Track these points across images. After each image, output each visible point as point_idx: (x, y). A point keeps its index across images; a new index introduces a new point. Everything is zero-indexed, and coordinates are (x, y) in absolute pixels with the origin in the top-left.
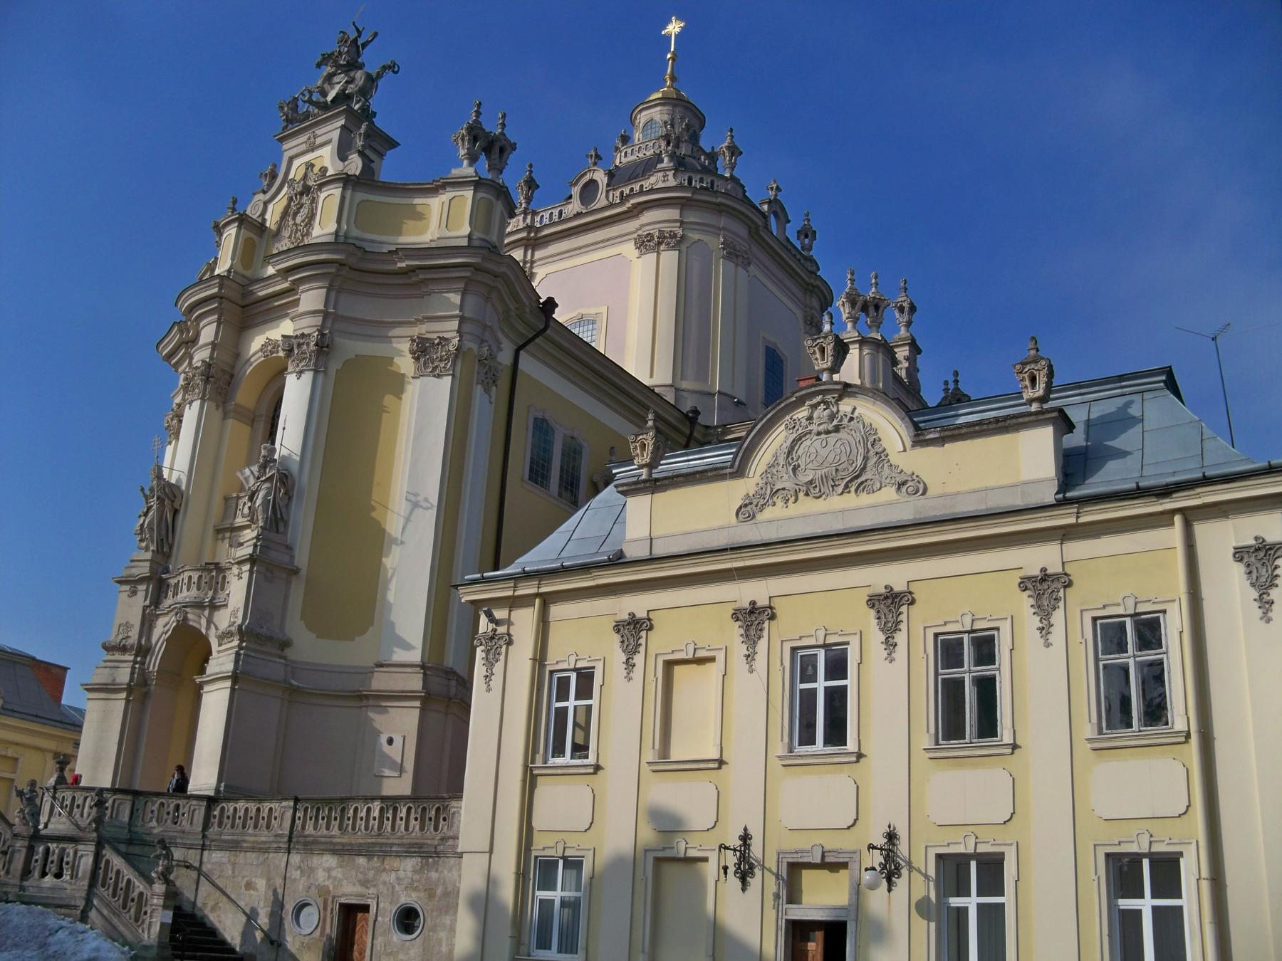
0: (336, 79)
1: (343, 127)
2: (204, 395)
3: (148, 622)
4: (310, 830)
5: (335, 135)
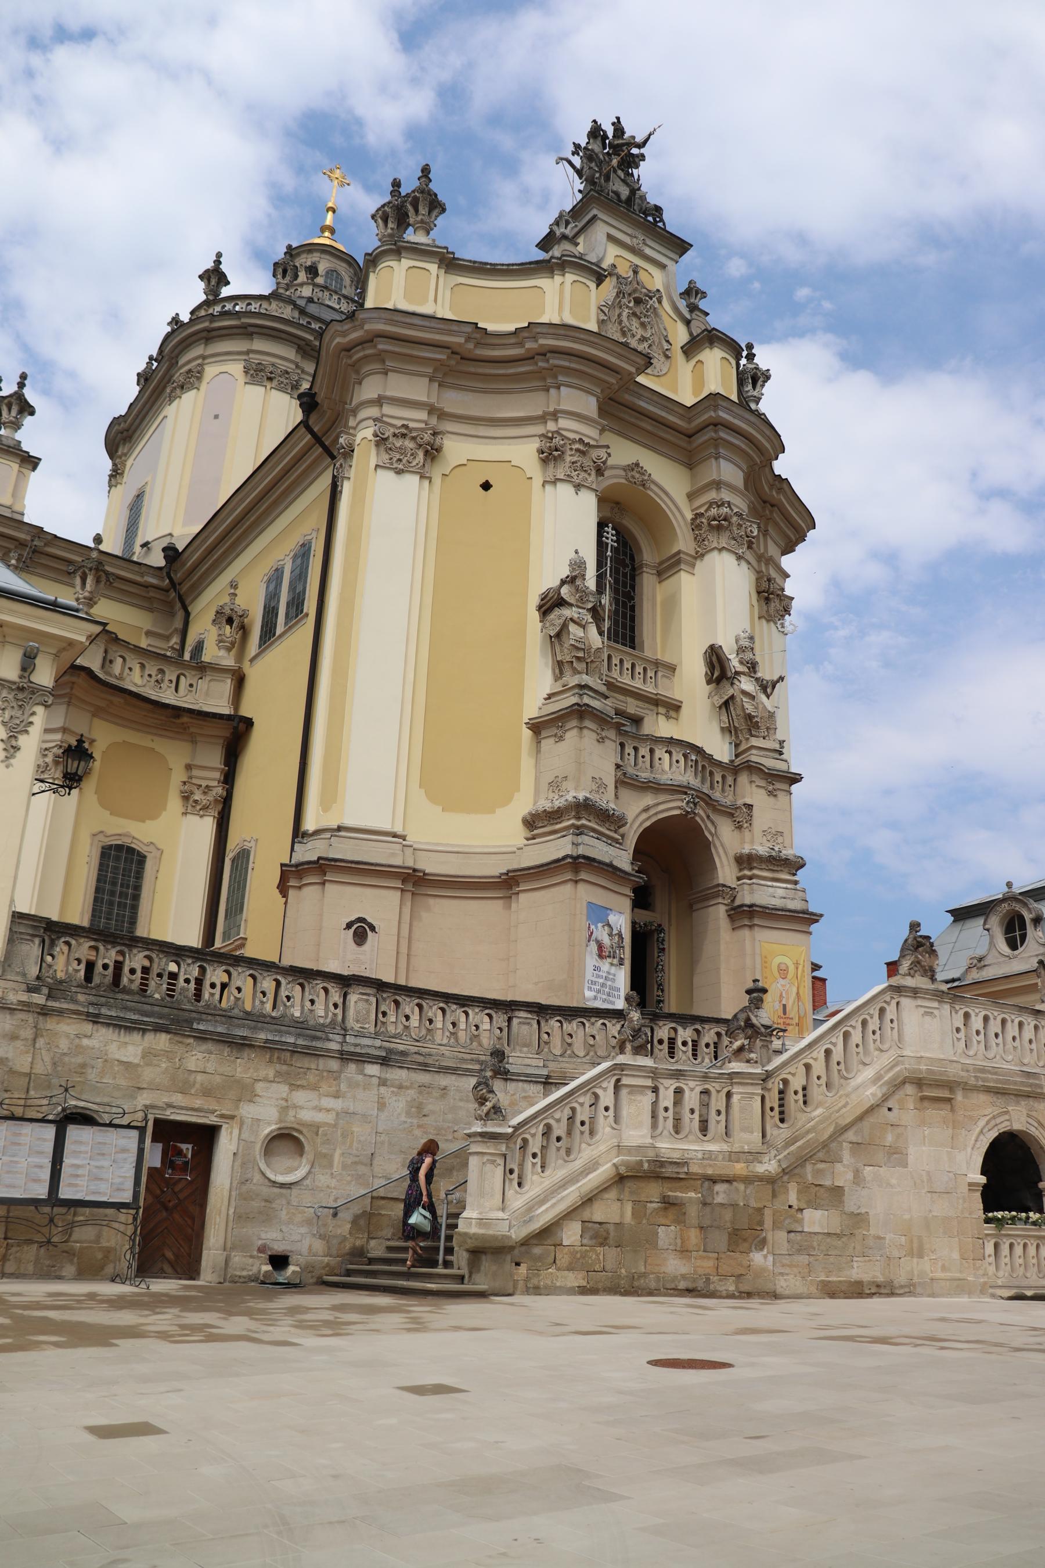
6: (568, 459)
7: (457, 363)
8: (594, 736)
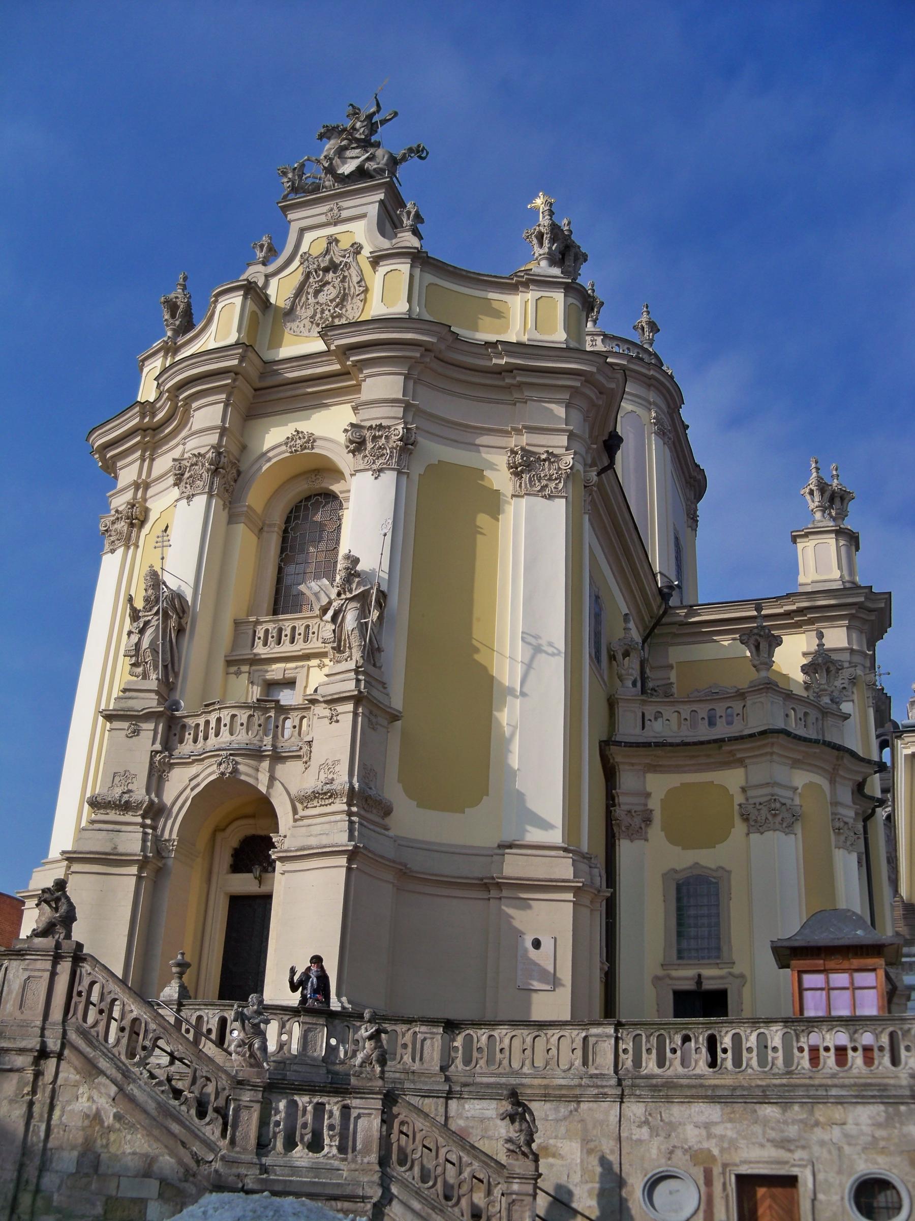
0: (349, 153)
1: (381, 202)
2: (211, 488)
3: (157, 775)
4: (650, 1065)
5: (373, 210)
6: (187, 475)
7: (153, 437)
8: (125, 732)
